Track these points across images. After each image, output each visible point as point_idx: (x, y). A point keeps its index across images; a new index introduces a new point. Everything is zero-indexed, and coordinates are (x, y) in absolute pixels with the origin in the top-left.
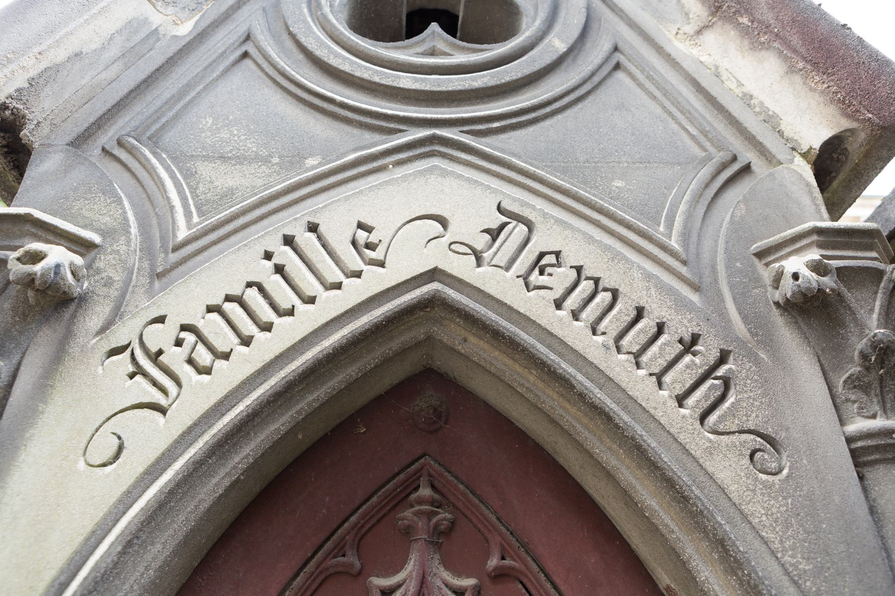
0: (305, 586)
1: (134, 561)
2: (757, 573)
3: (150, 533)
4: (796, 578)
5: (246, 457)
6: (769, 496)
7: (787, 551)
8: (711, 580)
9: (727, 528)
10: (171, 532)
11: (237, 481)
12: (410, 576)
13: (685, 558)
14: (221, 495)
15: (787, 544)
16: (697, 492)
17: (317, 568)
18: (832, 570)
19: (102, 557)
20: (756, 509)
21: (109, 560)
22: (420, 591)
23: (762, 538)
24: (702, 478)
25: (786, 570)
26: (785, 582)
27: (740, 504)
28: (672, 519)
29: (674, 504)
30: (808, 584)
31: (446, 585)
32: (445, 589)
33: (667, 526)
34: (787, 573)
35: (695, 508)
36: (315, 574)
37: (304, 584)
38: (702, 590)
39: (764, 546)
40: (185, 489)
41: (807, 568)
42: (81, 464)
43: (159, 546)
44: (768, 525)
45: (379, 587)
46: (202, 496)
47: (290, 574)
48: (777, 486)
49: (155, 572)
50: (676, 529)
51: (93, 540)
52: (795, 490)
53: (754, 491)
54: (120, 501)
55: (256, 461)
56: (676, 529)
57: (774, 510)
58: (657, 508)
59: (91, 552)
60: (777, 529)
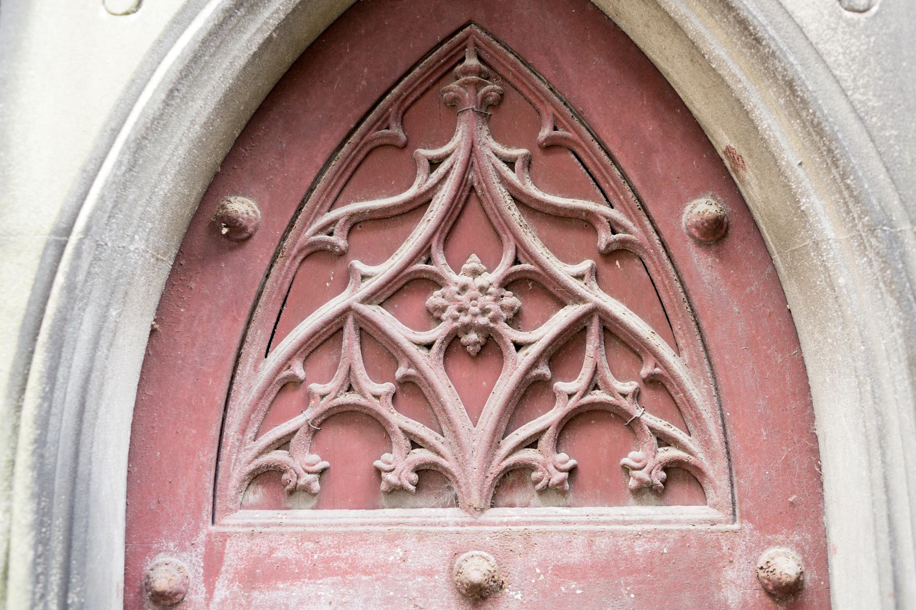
0: (351, 157)
1: (177, 116)
2: (822, 111)
3: (190, 87)
4: (863, 114)
5: (277, 11)
6: (851, 33)
7: (858, 89)
8: (773, 127)
9: (799, 68)
10: (210, 88)
11: (269, 39)
12: (458, 146)
13: (749, 108)
14: (255, 53)
15: (860, 82)
16: (772, 32)
17: (362, 139)
18: (902, 107)
19: (147, 103)
20: (833, 50)
21: (155, 107)
22: (469, 160)
23: (834, 76)
24: (780, 18)
25: (853, 107)
26: (851, 119)
27: (817, 43)
28: (741, 69)
29: (744, 50)
30: (874, 120)
31: (496, 155)
32: (494, 158)
33: (734, 75)
34: (854, 110)
35: (767, 50)
36: (360, 146)
37: (350, 154)
38: (762, 139)
39: (836, 85)
40: (218, 43)
41: (876, 105)
42: (103, 14)
43: (200, 102)
44: (843, 63)
45: (427, 157)
46: (235, 52)
47: (334, 144)
48: (862, 24)
49: (201, 127)
50: (743, 78)
51: (134, 88)
52: (881, 28)
53: (835, 29)
54: (153, 50)
55: (287, 18)
56: (743, 78)
57: (854, 49)
58: (726, 57)
59: (136, 100)
60: (853, 68)
